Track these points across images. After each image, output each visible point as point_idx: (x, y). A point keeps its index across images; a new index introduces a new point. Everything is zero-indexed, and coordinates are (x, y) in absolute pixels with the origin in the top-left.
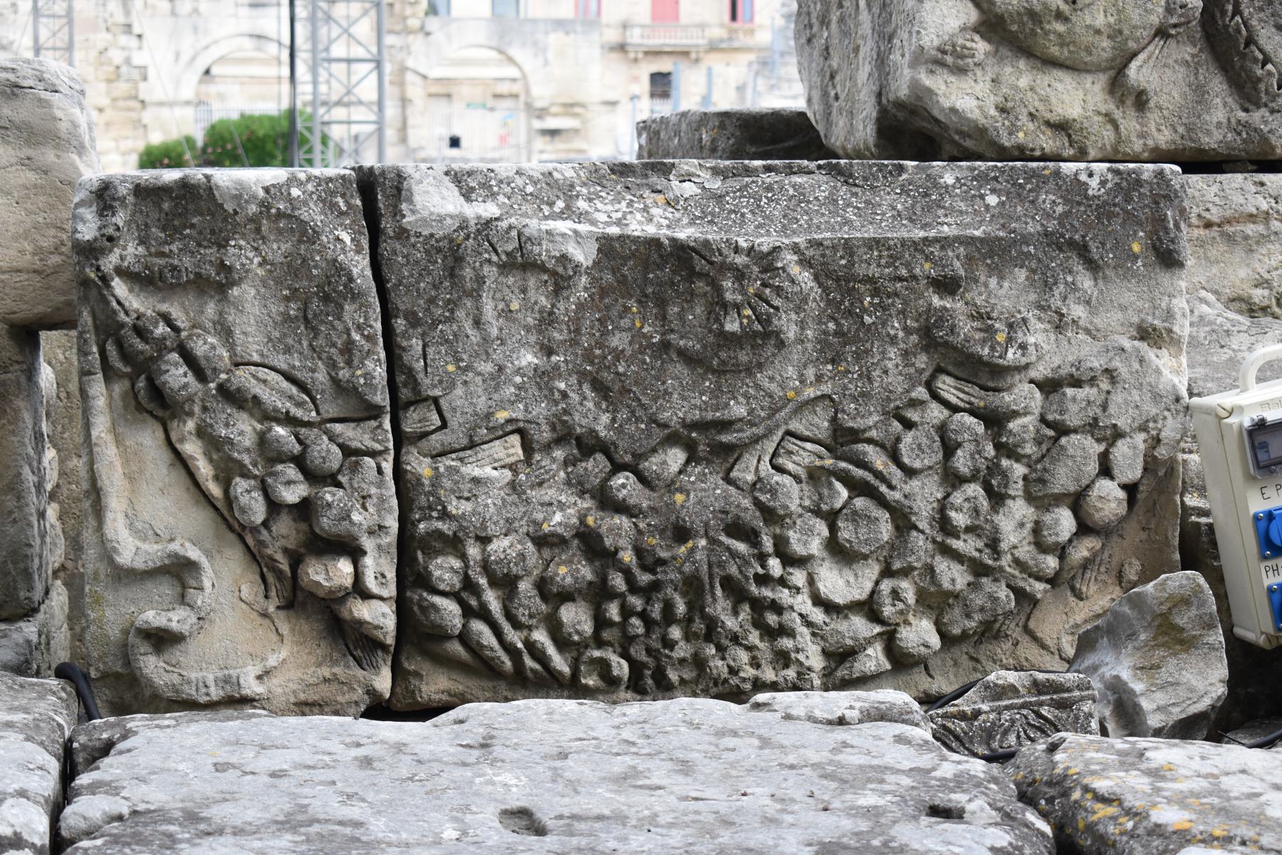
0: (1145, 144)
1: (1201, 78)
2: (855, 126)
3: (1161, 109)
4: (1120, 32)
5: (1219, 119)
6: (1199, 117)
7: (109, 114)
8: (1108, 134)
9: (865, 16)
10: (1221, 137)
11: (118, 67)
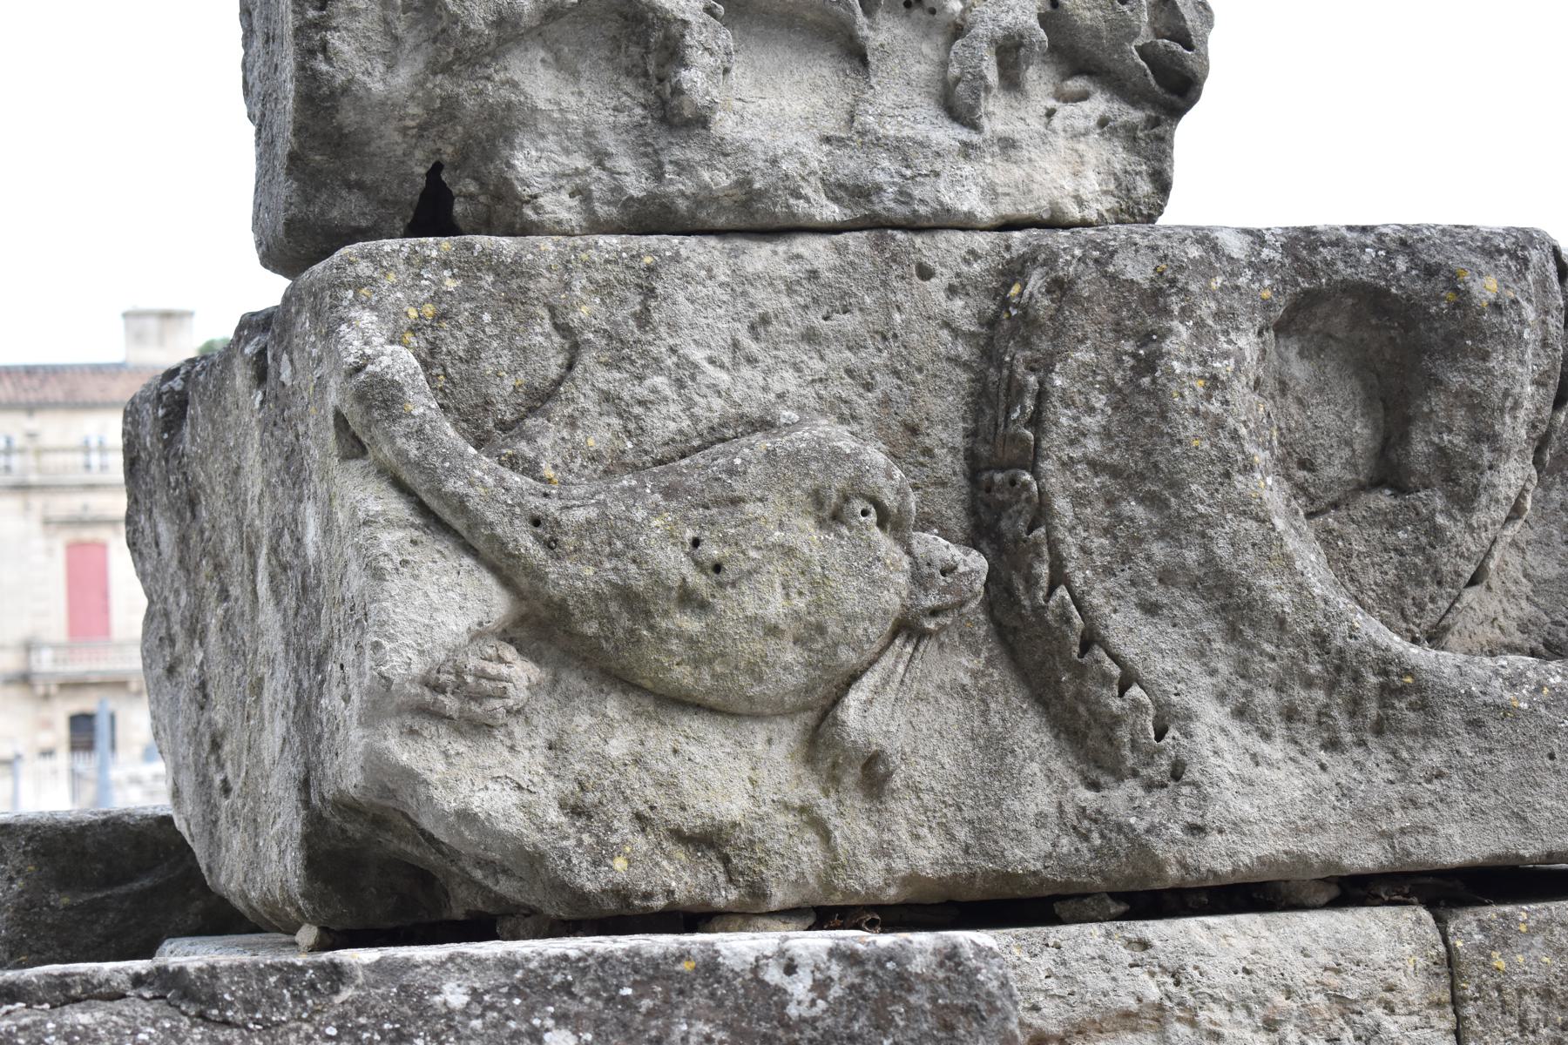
0: (889, 870)
1: (996, 720)
2: (261, 856)
3: (917, 791)
4: (821, 629)
5: (1040, 810)
6: (998, 805)
8: (809, 852)
9: (269, 616)
10: (1048, 847)
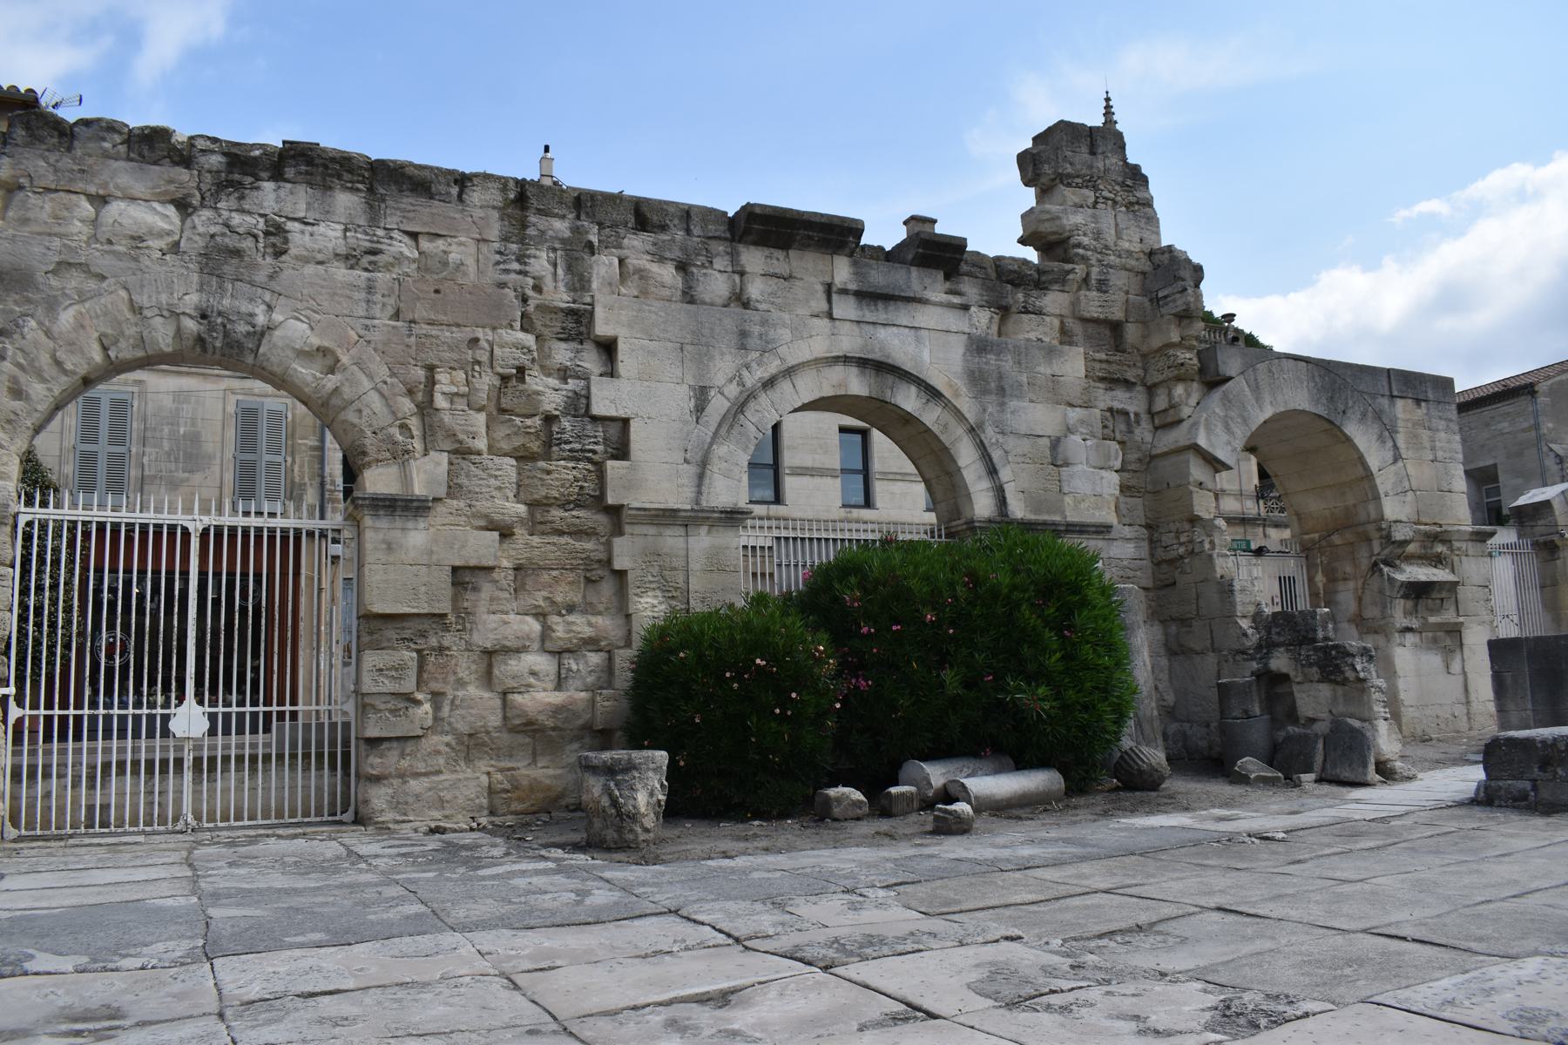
7: (526, 544)
11: (549, 419)
